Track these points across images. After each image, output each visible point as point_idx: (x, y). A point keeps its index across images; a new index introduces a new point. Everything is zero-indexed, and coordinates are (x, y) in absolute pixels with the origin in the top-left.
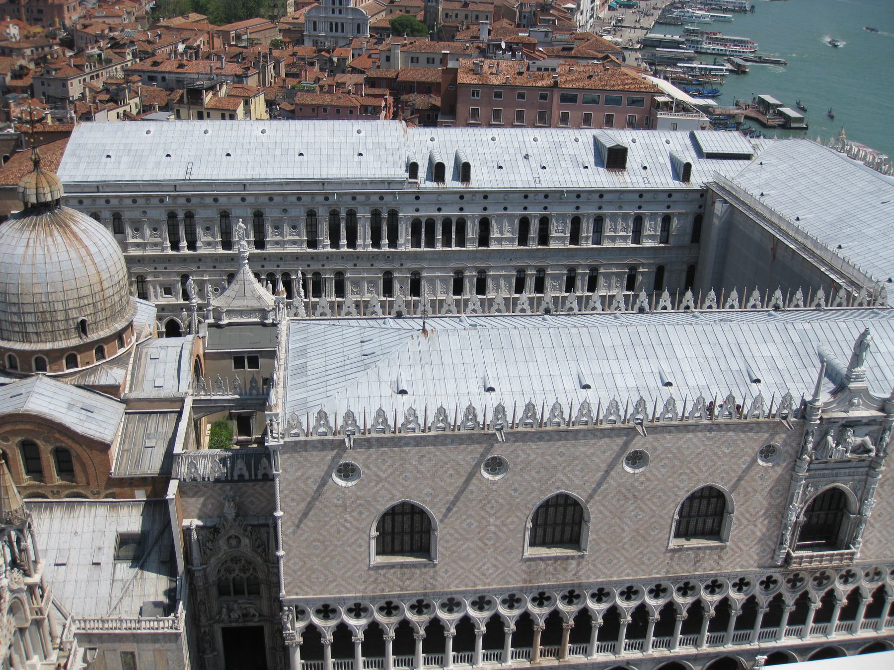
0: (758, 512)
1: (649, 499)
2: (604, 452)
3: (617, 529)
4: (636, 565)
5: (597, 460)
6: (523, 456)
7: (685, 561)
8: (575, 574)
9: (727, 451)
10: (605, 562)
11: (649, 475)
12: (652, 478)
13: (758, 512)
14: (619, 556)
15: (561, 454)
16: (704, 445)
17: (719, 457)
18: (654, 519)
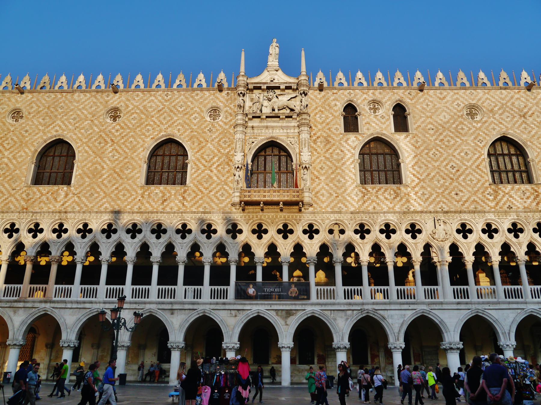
0: (212, 159)
1: (123, 143)
2: (91, 107)
3: (99, 167)
4: (113, 200)
5: (85, 112)
6: (35, 108)
7: (154, 200)
8: (63, 205)
9: (181, 110)
10: (87, 195)
11: (122, 125)
12: (125, 127)
13: (212, 159)
14: (98, 190)
15: (62, 108)
16: (163, 105)
17: (175, 114)
18: (127, 160)
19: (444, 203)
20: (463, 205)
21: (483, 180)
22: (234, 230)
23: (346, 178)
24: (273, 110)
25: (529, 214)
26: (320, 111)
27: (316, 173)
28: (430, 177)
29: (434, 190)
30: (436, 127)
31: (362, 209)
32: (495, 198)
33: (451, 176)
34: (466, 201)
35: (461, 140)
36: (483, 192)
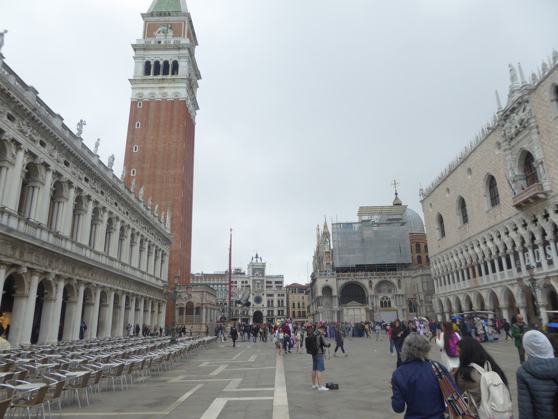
22: (525, 225)
24: (516, 127)
26: (540, 108)
27: (548, 163)
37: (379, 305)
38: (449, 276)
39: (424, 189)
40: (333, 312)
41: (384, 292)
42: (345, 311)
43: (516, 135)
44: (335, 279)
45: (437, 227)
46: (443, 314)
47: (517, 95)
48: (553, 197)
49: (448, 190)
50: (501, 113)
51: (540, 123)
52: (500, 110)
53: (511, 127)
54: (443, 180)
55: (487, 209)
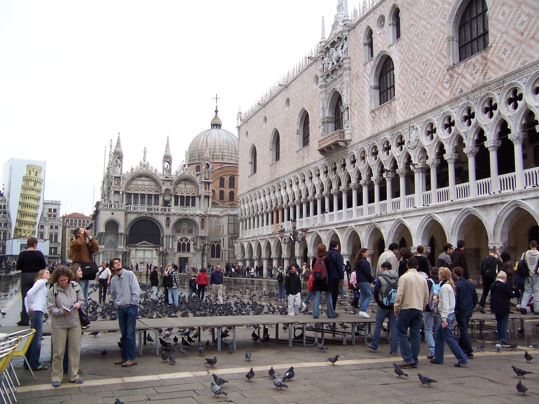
19: (416, 107)
20: (427, 104)
21: (443, 67)
22: (326, 172)
23: (366, 107)
25: (476, 92)
27: (353, 110)
28: (408, 83)
29: (410, 96)
30: (416, 22)
31: (373, 134)
32: (451, 84)
33: (422, 73)
34: (430, 99)
35: (431, 25)
36: (442, 82)
37: (176, 247)
38: (255, 217)
39: (243, 113)
40: (117, 252)
41: (183, 233)
42: (133, 252)
43: (332, 72)
44: (123, 213)
45: (250, 161)
46: (244, 261)
47: (340, 29)
48: (351, 146)
49: (265, 119)
50: (323, 44)
51: (352, 65)
52: (323, 40)
53: (329, 63)
54: (263, 106)
55: (297, 148)
